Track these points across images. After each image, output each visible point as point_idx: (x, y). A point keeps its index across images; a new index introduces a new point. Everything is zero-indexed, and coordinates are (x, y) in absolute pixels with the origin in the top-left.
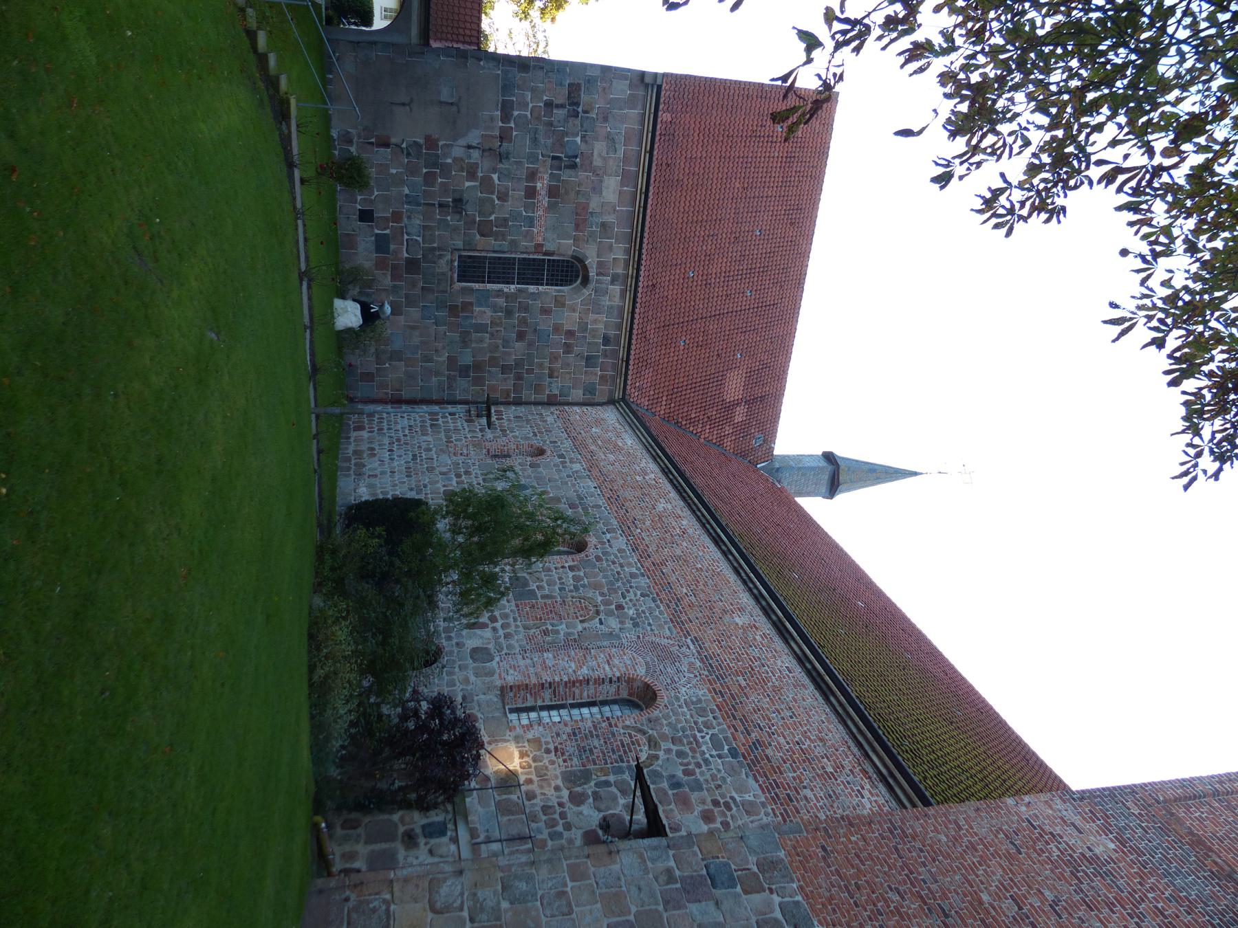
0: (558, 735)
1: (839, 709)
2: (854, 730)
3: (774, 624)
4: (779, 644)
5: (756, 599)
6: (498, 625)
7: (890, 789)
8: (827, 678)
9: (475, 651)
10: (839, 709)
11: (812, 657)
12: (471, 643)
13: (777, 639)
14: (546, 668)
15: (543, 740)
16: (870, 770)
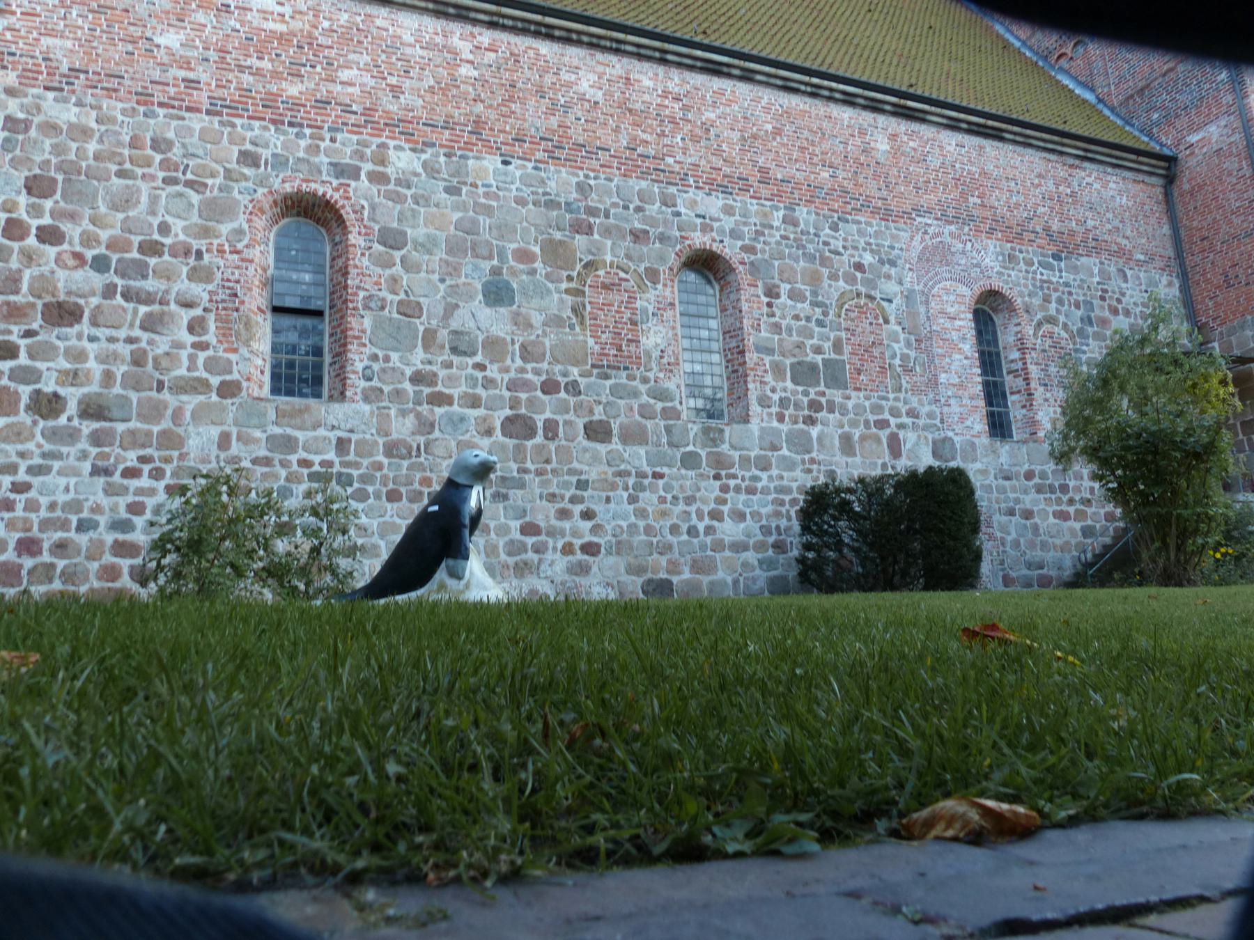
0: (1046, 400)
2: (1041, 144)
3: (894, 114)
4: (926, 131)
6: (893, 421)
8: (990, 123)
9: (935, 454)
11: (962, 116)
13: (915, 126)
14: (960, 386)
16: (1071, 161)
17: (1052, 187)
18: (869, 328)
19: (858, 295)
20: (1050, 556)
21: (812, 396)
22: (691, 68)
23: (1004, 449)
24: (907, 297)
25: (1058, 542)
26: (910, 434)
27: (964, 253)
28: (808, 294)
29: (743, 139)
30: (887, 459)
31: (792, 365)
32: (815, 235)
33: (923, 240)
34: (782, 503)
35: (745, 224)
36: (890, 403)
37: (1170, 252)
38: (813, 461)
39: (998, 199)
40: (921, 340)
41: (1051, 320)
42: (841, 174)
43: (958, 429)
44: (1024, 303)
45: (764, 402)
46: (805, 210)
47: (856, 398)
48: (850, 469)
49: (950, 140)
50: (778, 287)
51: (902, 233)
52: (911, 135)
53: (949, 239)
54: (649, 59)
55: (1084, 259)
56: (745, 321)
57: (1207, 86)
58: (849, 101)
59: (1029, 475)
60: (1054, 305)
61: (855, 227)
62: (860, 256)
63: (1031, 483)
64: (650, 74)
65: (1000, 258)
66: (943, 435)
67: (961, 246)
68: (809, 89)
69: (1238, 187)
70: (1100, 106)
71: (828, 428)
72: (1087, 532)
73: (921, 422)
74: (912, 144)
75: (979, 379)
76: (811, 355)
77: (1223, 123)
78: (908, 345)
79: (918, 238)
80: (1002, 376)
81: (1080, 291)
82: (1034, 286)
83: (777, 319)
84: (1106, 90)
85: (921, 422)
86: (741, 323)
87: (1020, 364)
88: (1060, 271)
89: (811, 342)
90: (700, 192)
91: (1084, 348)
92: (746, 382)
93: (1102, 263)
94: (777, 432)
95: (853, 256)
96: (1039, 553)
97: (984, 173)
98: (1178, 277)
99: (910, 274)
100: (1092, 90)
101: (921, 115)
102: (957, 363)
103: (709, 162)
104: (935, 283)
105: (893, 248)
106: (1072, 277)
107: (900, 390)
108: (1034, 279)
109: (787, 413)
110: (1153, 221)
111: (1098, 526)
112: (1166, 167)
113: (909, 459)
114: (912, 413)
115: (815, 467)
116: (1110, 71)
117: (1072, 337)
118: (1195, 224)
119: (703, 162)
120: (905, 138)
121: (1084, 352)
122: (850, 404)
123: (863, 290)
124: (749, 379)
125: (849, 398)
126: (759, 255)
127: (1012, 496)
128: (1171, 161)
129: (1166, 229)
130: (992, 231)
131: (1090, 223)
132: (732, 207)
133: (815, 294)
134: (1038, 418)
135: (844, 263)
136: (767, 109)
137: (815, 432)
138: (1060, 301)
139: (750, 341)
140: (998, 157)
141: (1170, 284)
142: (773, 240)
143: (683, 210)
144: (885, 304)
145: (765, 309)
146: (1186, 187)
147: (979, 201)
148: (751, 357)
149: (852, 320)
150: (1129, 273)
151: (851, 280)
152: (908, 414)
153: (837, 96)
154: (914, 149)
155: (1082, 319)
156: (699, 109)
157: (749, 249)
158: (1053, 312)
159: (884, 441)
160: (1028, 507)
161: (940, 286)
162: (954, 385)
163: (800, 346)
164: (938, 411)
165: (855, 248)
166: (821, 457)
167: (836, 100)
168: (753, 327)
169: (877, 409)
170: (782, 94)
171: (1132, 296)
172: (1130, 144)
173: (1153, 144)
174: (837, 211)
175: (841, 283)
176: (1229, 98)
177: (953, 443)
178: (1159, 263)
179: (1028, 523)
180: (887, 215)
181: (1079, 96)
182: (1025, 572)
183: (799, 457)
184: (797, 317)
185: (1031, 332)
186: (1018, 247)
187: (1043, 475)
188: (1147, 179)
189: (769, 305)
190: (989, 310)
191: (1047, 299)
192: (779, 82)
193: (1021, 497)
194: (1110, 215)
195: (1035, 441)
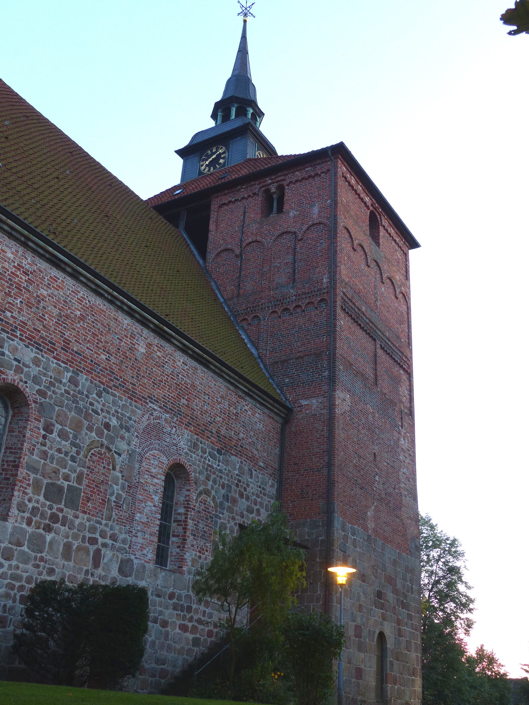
1: (217, 370)
2: (228, 378)
3: (154, 331)
4: (169, 348)
5: (132, 316)
6: (100, 540)
7: (251, 397)
10: (217, 370)
12: (114, 572)
13: (163, 343)
14: (146, 524)
15: (194, 557)
16: (240, 393)
17: (227, 407)
18: (102, 471)
19: (102, 445)
20: (171, 656)
21: (54, 511)
22: (41, 256)
23: (162, 575)
24: (130, 455)
25: (178, 646)
26: (108, 552)
27: (170, 434)
28: (71, 436)
29: (60, 315)
30: (90, 567)
31: (47, 483)
32: (87, 396)
33: (149, 419)
34: (12, 587)
35: (45, 375)
36: (102, 527)
37: (276, 466)
38: (42, 559)
39: (197, 404)
40: (131, 487)
41: (207, 492)
42: (113, 359)
43: (138, 554)
44: (195, 477)
45: (21, 508)
46: (85, 376)
47: (82, 518)
48: (71, 572)
49: (180, 358)
50: (54, 425)
51: (138, 411)
52: (160, 347)
53: (164, 423)
54: (16, 239)
55: (233, 457)
56: (25, 444)
57: (317, 376)
58: (130, 313)
59: (172, 596)
60: (211, 483)
61: (112, 398)
62: (110, 419)
63: (171, 602)
64: (13, 250)
65: (189, 444)
66: (128, 557)
67: (170, 429)
68: (109, 297)
69: (319, 440)
70: (259, 360)
71: (57, 537)
72: (196, 642)
73: (117, 545)
74: (158, 353)
75: (158, 522)
76: (62, 480)
77: (320, 401)
78: (123, 488)
79: (146, 416)
80: (170, 523)
81: (226, 477)
82: (203, 467)
83: (46, 448)
84: (264, 352)
85: (117, 545)
86: (22, 445)
87: (184, 517)
88: (219, 461)
89: (64, 471)
90: (21, 343)
91: (221, 515)
92: (13, 489)
93: (242, 463)
94: (25, 532)
95: (105, 418)
96: (165, 653)
97: (193, 385)
98: (277, 482)
99: (136, 439)
100: (257, 349)
101: (169, 337)
102: (148, 508)
103: (33, 324)
104: (149, 450)
105: (130, 419)
106: (225, 467)
107: (110, 520)
108: (204, 462)
109: (34, 519)
110: (272, 443)
111: (202, 638)
112: (285, 413)
113: (103, 570)
114: (114, 537)
115: (42, 564)
116: (269, 342)
117: (216, 507)
118: (293, 453)
119: (30, 323)
120: (156, 349)
121: (220, 518)
122: (77, 522)
123: (106, 443)
124: (16, 488)
125: (77, 517)
126: (47, 400)
127: (159, 609)
128: (290, 411)
129: (277, 451)
130: (188, 425)
131: (241, 435)
132: (39, 360)
133: (75, 437)
134: (186, 557)
135: (99, 421)
136: (80, 301)
137: (49, 537)
138: (215, 481)
139: (25, 460)
140: (204, 379)
141: (272, 486)
142: (59, 391)
143: (7, 352)
144: (116, 456)
145: (41, 439)
146: (293, 429)
147: (186, 403)
148: (22, 472)
149: (94, 462)
150: (254, 473)
151: (100, 434)
152: (110, 537)
153: (125, 308)
154: (159, 357)
155: (223, 496)
156: (38, 285)
157: (41, 393)
158: (209, 488)
159: (92, 553)
160: (166, 618)
161: (151, 452)
162: (143, 523)
163: (56, 472)
164: (129, 539)
165: (108, 412)
166: (49, 557)
167: (123, 310)
168: (29, 449)
169: (93, 529)
170: (92, 294)
171: (252, 488)
172: (271, 393)
173: (282, 396)
174: (103, 384)
175: (94, 434)
176: (325, 388)
177: (133, 565)
178: (270, 471)
179: (163, 629)
180: (132, 396)
181: (248, 348)
182: (154, 665)
183: (34, 554)
184: (59, 451)
185: (195, 498)
186: (200, 439)
187: (179, 598)
188: (275, 417)
189: (44, 437)
190: (176, 474)
191: (208, 478)
192: (93, 286)
193: (164, 610)
194: (252, 433)
195: (180, 573)
